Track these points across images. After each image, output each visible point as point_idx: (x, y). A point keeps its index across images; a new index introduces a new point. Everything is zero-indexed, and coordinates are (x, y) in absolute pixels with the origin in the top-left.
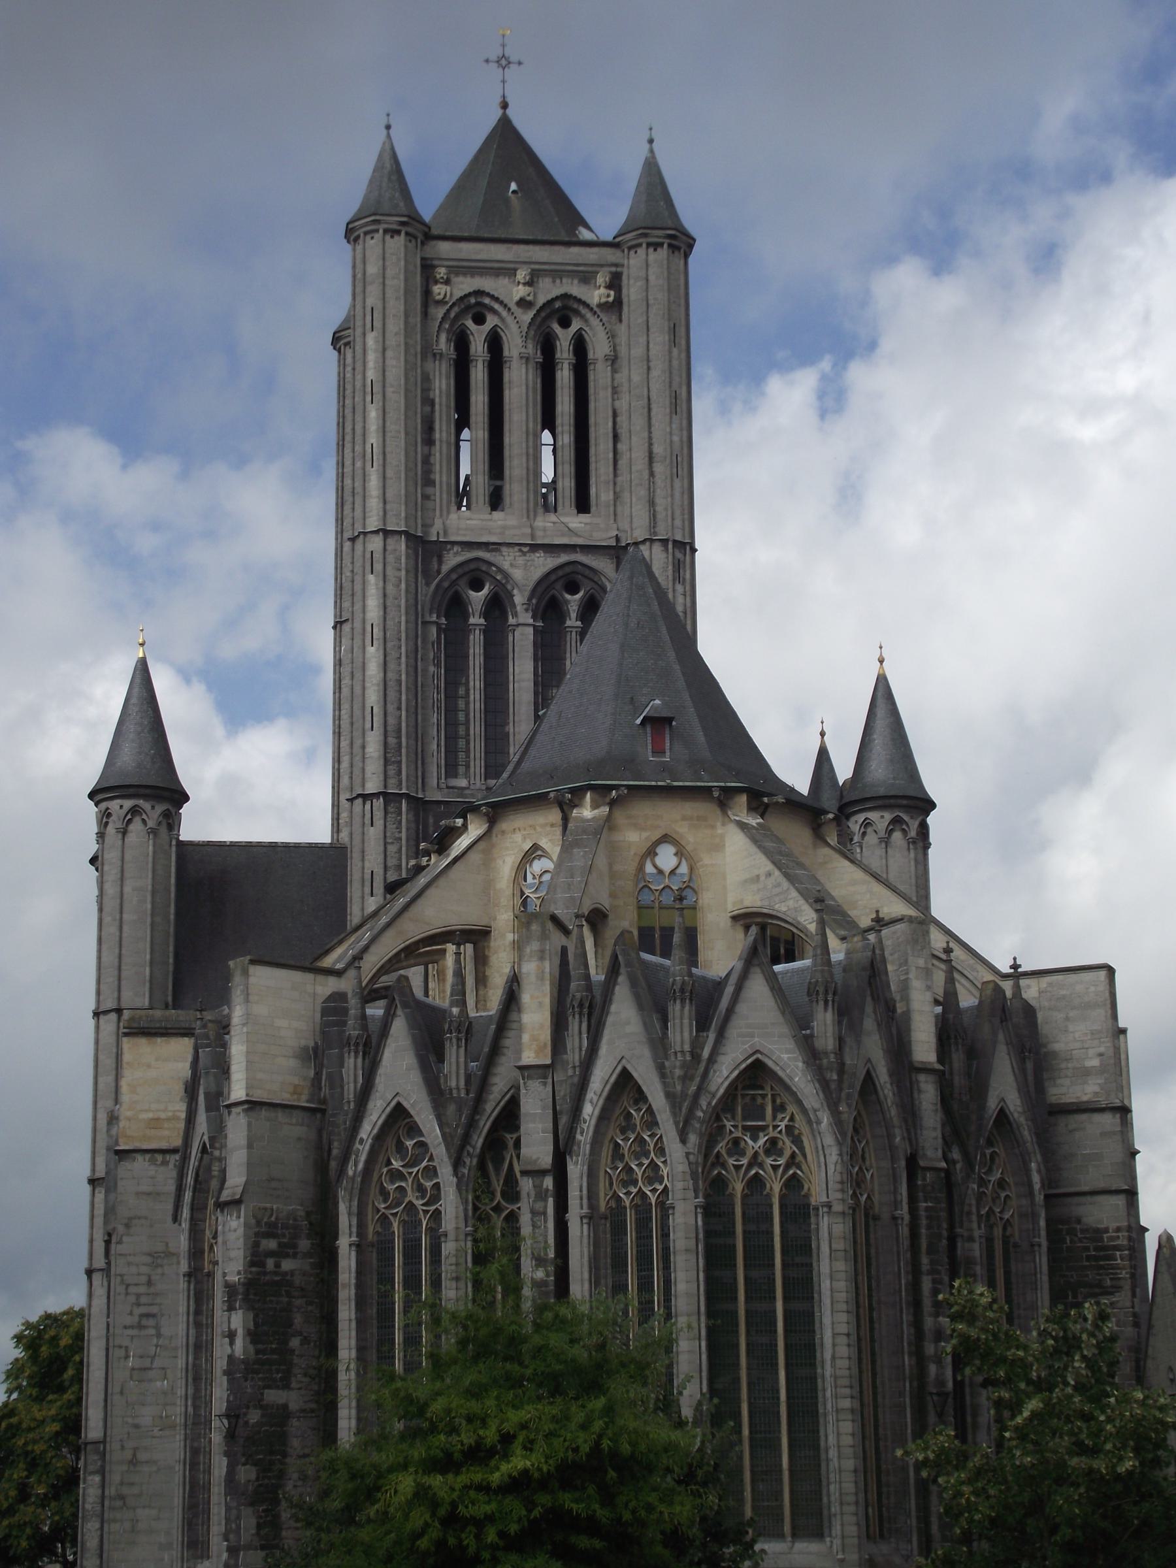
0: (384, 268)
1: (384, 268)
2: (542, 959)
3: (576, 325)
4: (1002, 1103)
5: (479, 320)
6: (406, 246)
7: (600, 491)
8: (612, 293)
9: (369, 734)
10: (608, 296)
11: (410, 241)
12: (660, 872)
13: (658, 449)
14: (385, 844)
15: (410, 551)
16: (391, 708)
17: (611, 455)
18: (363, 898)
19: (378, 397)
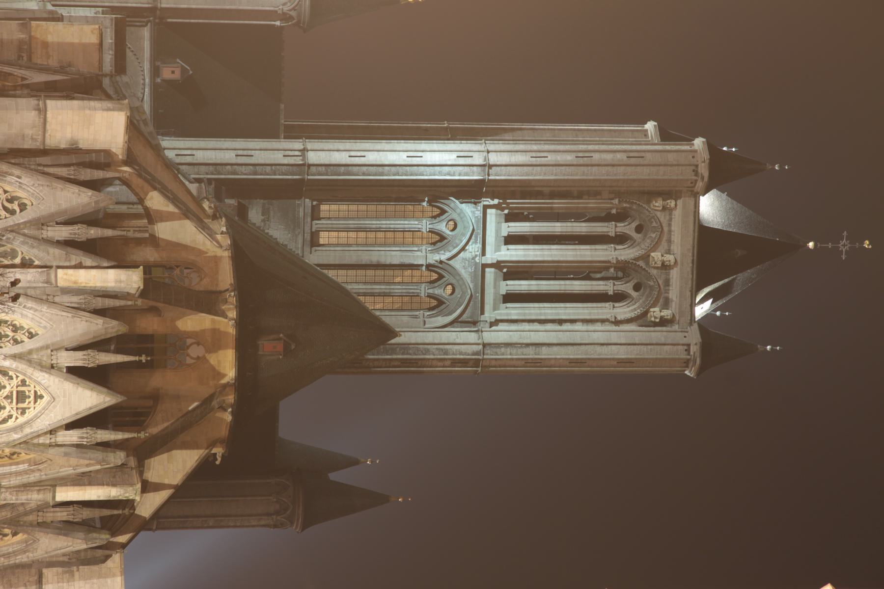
0: (672, 165)
1: (672, 165)
2: (116, 281)
3: (634, 294)
4: (37, 541)
5: (639, 229)
6: (687, 180)
7: (515, 310)
8: (658, 320)
9: (348, 154)
10: (656, 318)
11: (692, 183)
12: (188, 347)
13: (544, 349)
14: (271, 165)
15: (473, 182)
16: (365, 168)
17: (543, 317)
18: (235, 150)
19: (581, 161)
